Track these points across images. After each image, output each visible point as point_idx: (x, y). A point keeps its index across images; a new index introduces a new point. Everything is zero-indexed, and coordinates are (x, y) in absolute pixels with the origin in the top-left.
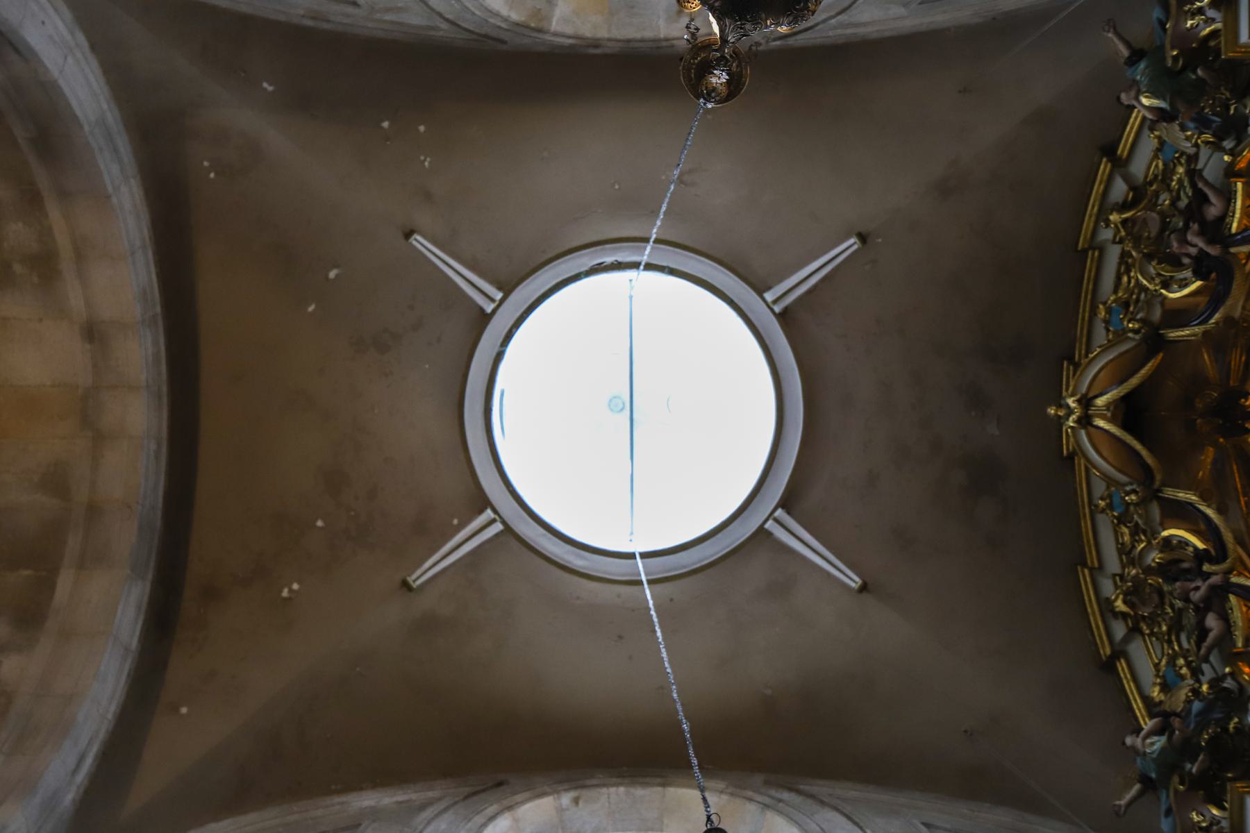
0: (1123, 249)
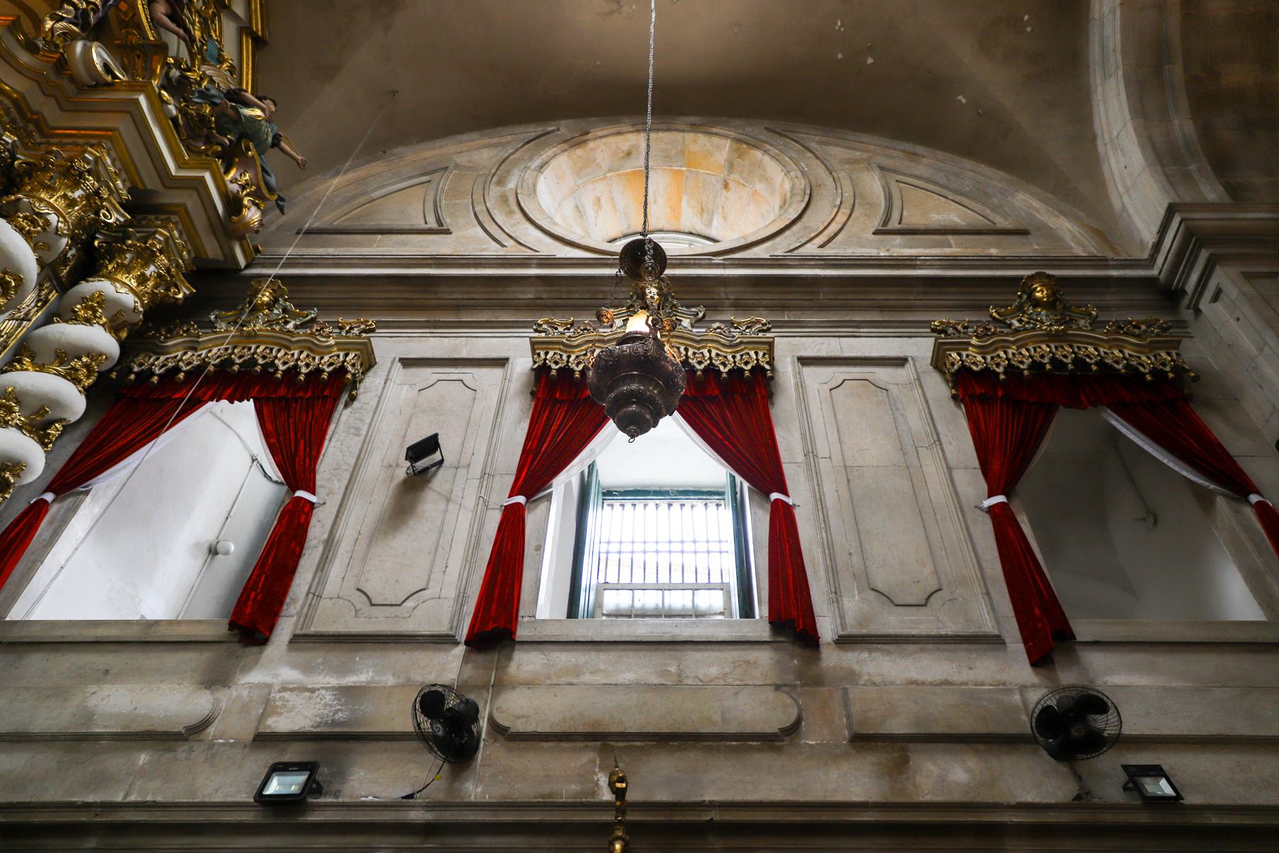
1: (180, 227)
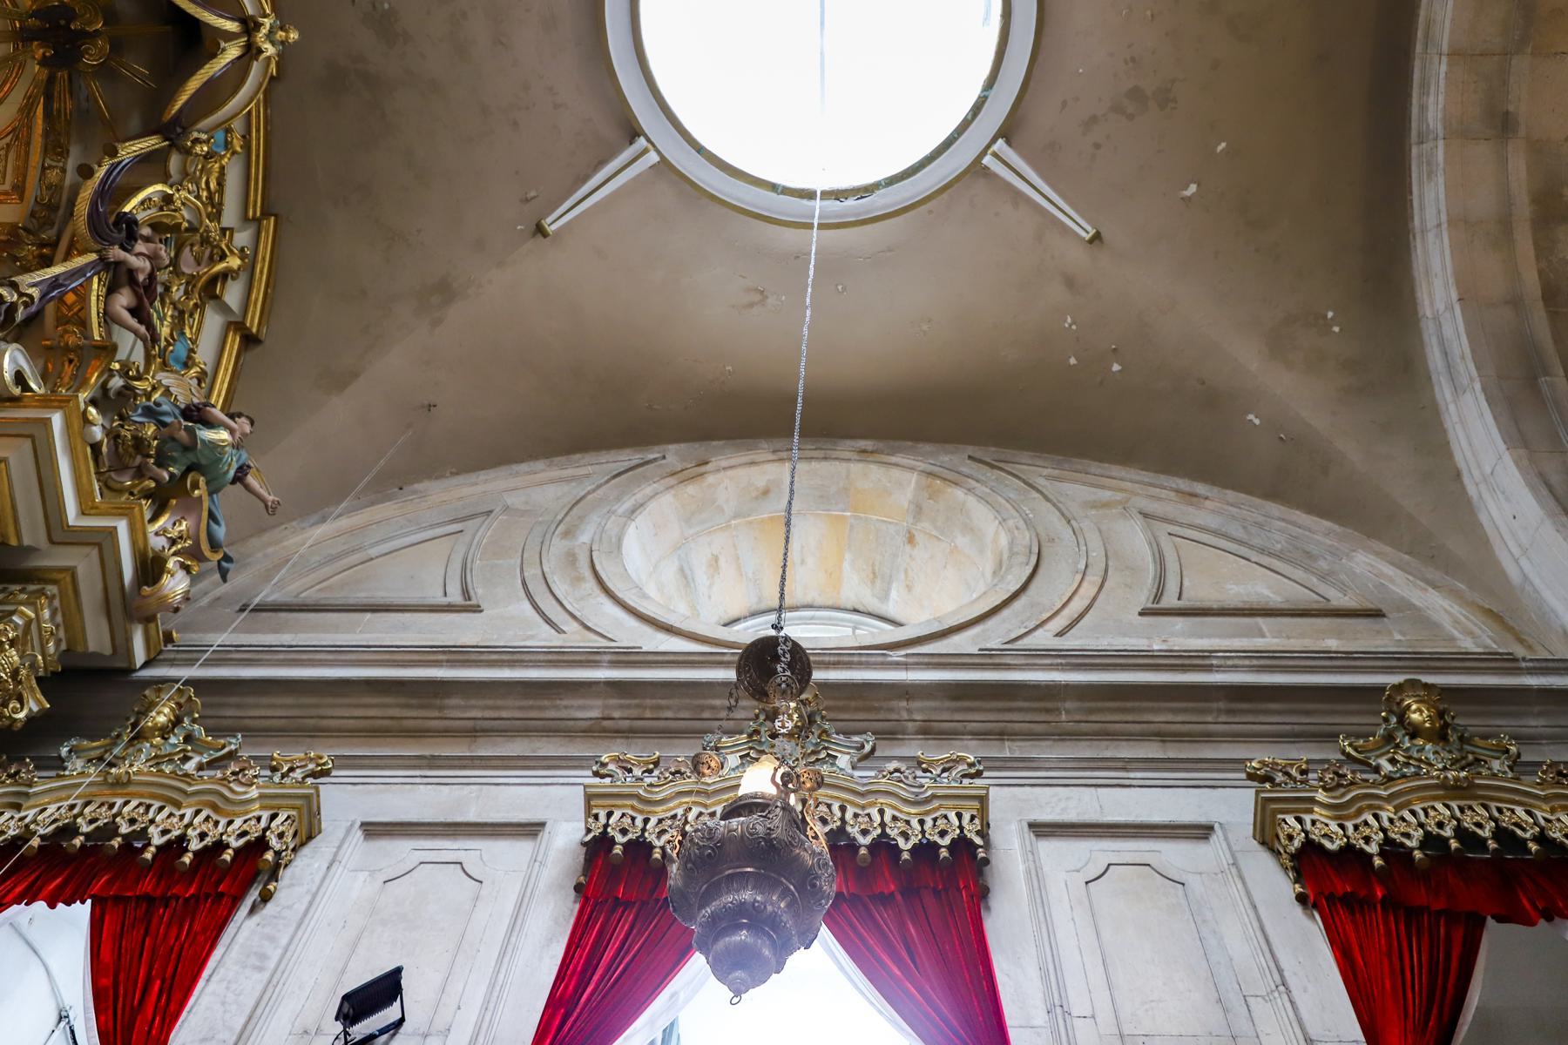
0: (219, 223)
1: (57, 603)
